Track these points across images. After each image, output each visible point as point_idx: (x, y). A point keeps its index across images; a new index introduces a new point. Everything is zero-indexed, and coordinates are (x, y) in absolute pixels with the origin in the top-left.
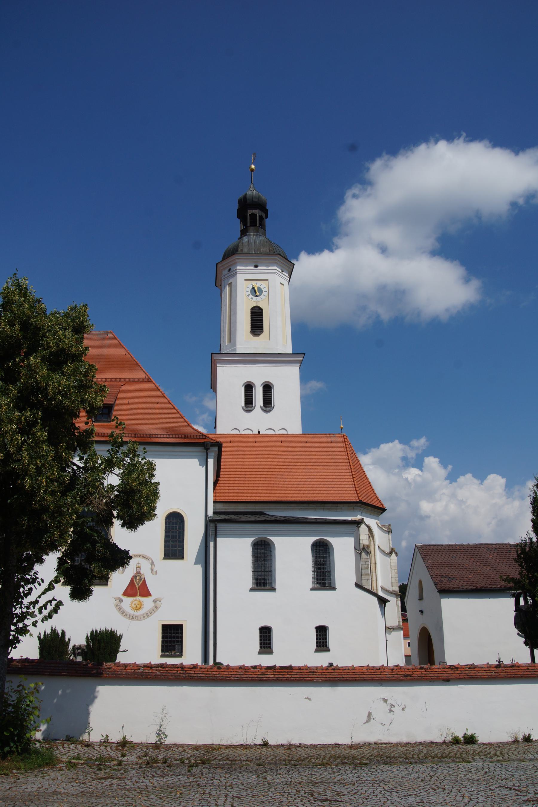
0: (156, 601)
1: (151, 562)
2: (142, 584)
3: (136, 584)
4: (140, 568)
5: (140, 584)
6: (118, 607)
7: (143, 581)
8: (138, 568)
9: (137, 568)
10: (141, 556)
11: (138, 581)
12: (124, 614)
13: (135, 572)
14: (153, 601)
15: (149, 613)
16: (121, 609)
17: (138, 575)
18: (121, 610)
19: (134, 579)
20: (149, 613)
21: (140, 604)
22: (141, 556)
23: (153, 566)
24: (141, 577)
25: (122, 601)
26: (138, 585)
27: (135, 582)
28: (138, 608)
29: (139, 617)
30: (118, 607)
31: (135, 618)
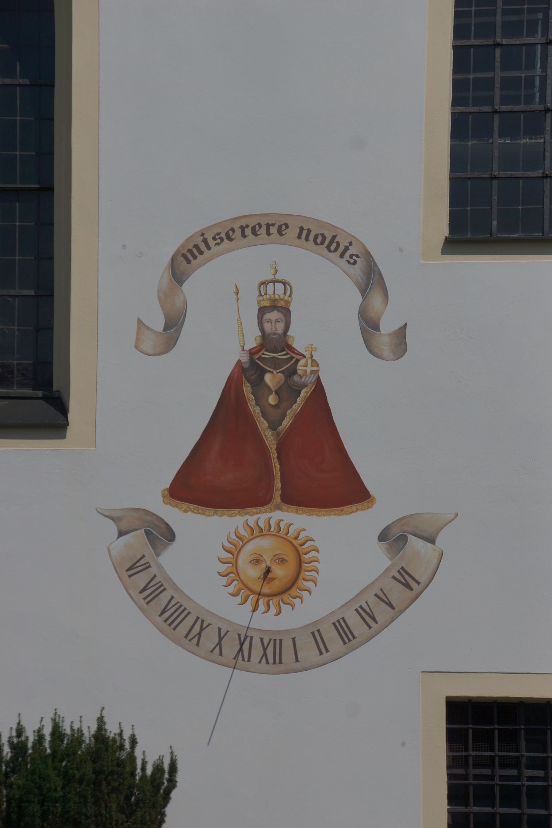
0: (402, 539)
1: (358, 270)
2: (298, 418)
3: (262, 424)
4: (286, 312)
5: (286, 423)
6: (142, 579)
7: (309, 400)
8: (274, 315)
9: (262, 311)
10: (292, 233)
11: (272, 400)
12: (183, 629)
13: (252, 343)
14: (383, 537)
15: (354, 621)
16: (160, 589)
17: (275, 364)
18: (164, 598)
19: (247, 389)
20: (354, 621)
21: (291, 558)
22: (292, 233)
23: (376, 301)
24: (293, 372)
25: (170, 536)
26: (274, 426)
27: (255, 410)
28: (276, 585)
29: (287, 645)
30: (142, 579)
31: (257, 653)
